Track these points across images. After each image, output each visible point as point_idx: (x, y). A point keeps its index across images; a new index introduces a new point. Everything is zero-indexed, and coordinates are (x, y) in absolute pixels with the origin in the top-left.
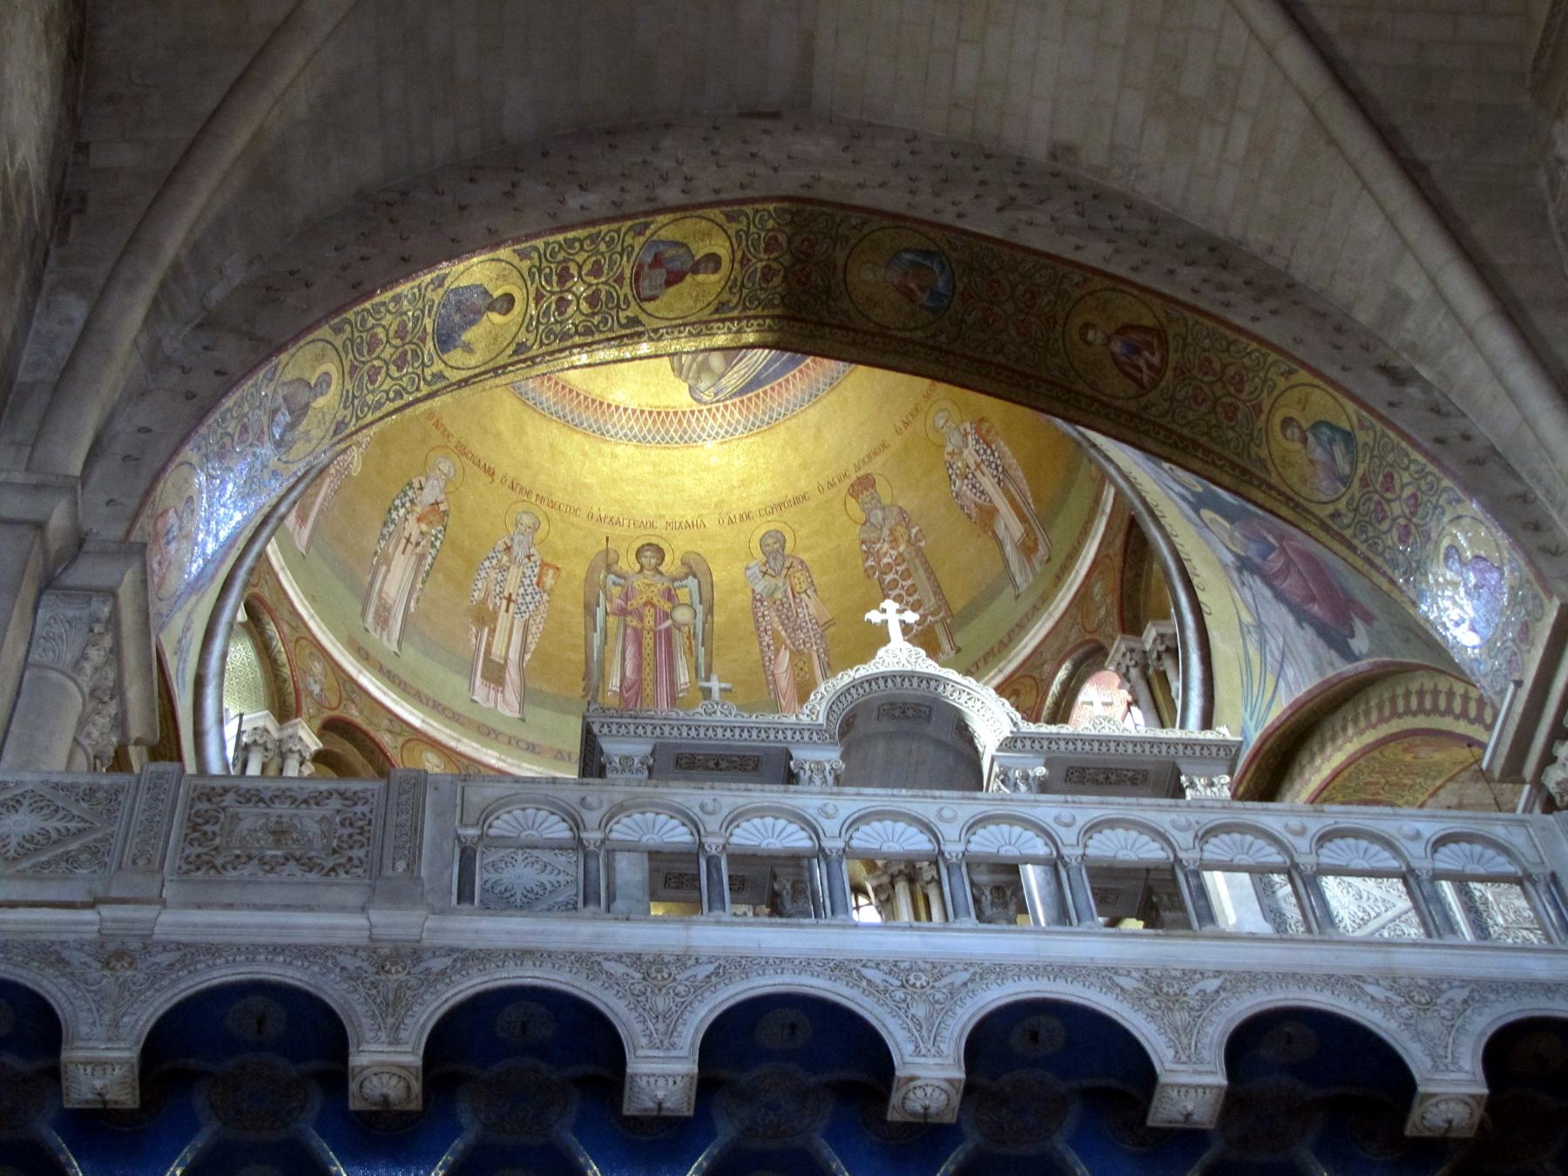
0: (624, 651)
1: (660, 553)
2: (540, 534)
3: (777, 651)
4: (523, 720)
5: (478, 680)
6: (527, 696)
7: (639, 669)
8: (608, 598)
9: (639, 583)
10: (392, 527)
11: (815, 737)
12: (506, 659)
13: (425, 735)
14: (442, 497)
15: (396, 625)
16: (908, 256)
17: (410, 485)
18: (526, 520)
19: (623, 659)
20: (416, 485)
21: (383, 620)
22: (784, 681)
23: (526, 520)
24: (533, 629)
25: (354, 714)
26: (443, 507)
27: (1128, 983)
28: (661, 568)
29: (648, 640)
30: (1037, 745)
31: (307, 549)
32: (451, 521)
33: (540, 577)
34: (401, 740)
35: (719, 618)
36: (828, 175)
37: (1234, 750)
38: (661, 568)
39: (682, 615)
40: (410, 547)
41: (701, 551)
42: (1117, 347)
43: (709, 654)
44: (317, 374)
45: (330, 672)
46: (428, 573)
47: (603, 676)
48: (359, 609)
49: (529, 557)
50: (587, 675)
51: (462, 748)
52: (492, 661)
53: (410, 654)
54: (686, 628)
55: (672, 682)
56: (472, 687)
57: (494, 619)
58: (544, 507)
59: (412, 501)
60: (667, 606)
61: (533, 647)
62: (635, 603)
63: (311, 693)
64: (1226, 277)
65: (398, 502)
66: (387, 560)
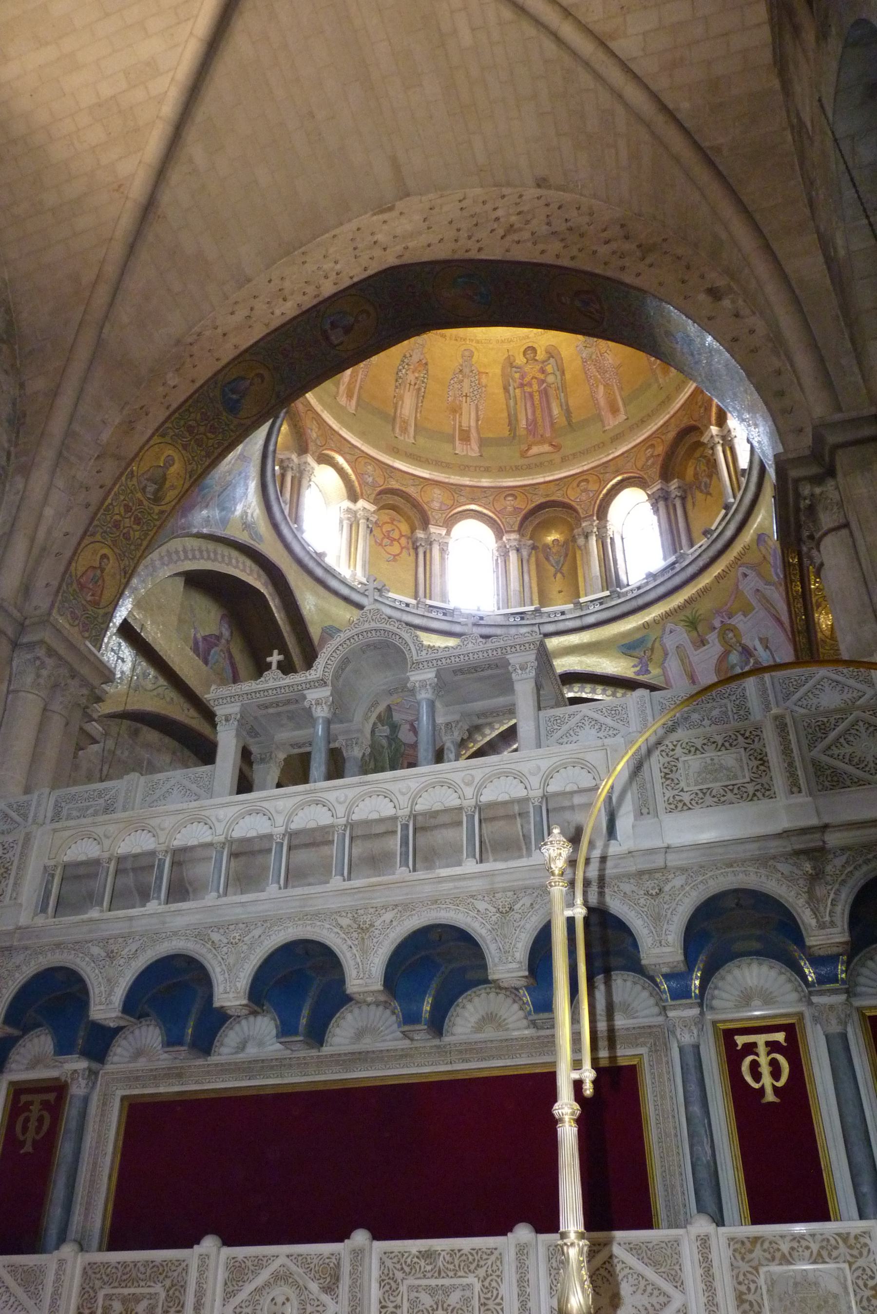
0: (525, 406)
1: (533, 349)
2: (474, 359)
3: (597, 386)
4: (481, 456)
5: (457, 442)
6: (483, 443)
7: (534, 412)
8: (514, 381)
9: (527, 369)
10: (400, 381)
11: (317, 684)
12: (469, 427)
13: (433, 481)
14: (422, 357)
15: (412, 430)
16: (459, 280)
17: (405, 356)
18: (467, 353)
19: (526, 409)
20: (408, 355)
21: (404, 430)
22: (602, 402)
23: (467, 353)
24: (481, 407)
25: (394, 485)
26: (424, 362)
27: (345, 922)
28: (537, 358)
29: (536, 396)
30: (430, 664)
31: (356, 410)
32: (430, 367)
33: (479, 379)
34: (420, 487)
35: (568, 376)
36: (411, 244)
37: (538, 643)
38: (537, 358)
39: (551, 379)
40: (412, 387)
41: (553, 344)
42: (578, 304)
43: (566, 396)
44: (162, 459)
45: (377, 467)
46: (423, 397)
47: (517, 420)
48: (391, 428)
49: (472, 371)
50: (510, 424)
51: (452, 481)
52: (463, 430)
53: (421, 441)
54: (553, 386)
55: (551, 415)
56: (454, 449)
57: (461, 409)
58: (475, 344)
59: (407, 364)
60: (542, 377)
61: (482, 417)
62: (527, 380)
63: (367, 483)
64: (627, 246)
65: (401, 367)
66: (401, 398)
